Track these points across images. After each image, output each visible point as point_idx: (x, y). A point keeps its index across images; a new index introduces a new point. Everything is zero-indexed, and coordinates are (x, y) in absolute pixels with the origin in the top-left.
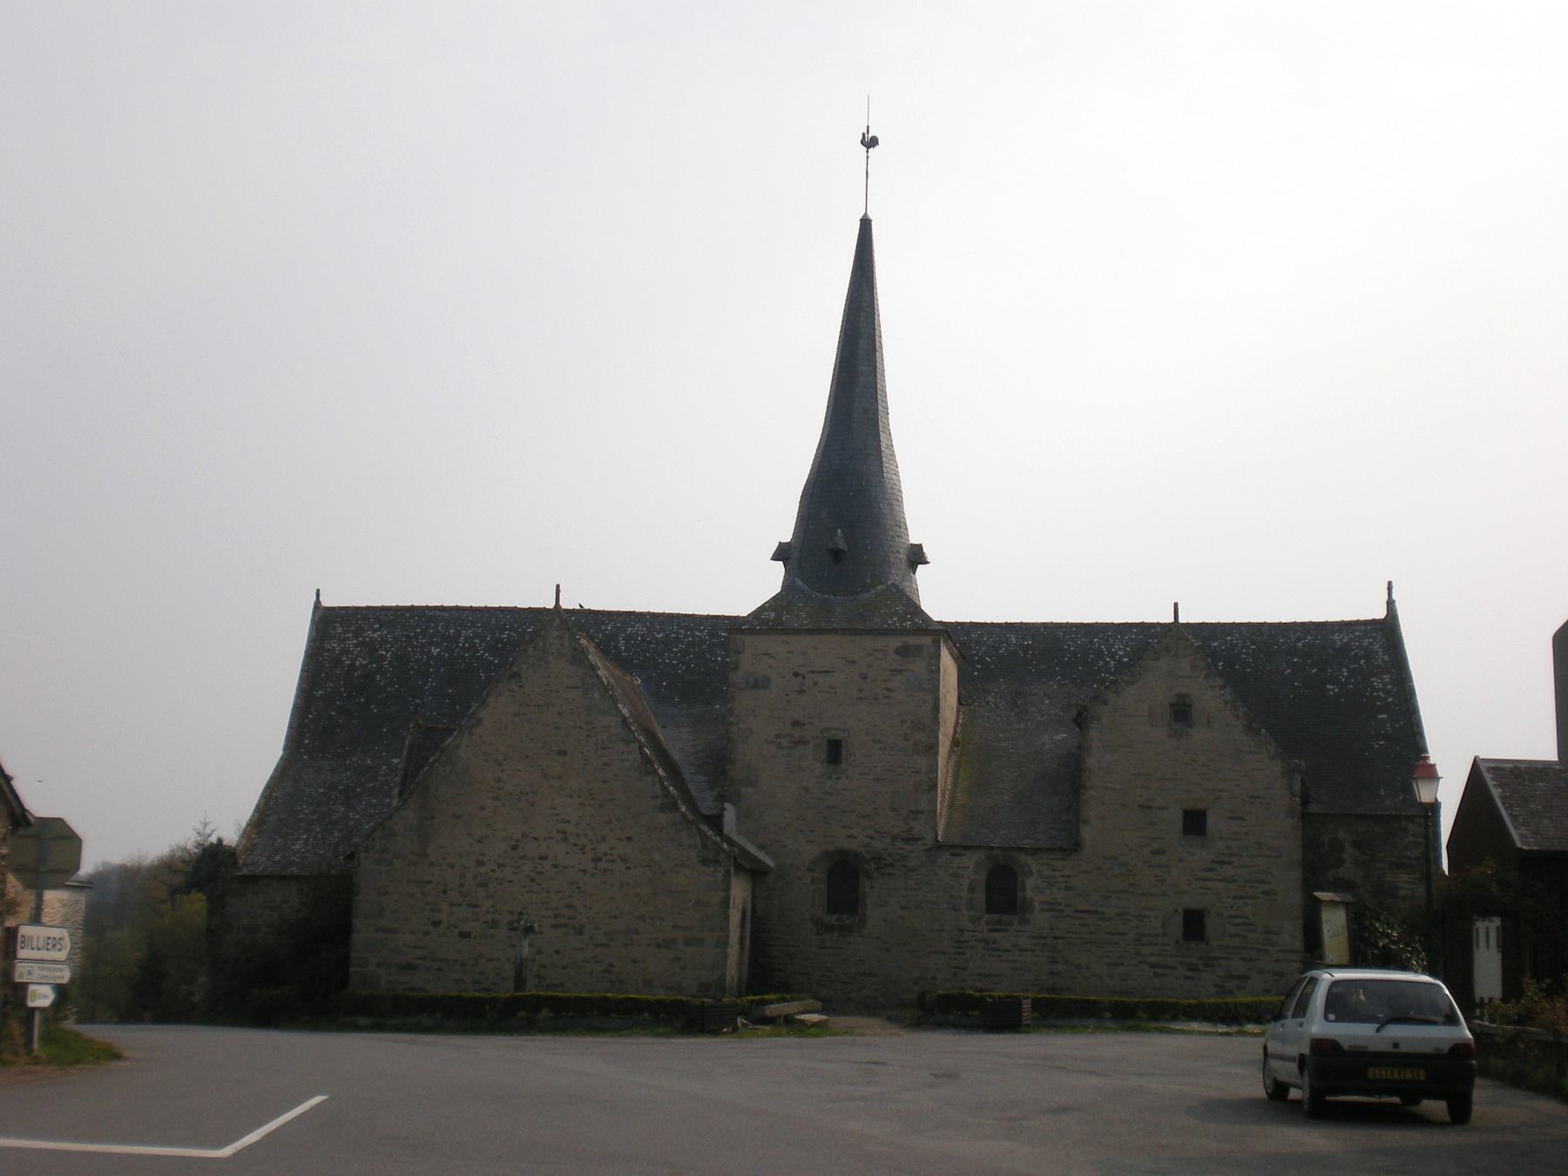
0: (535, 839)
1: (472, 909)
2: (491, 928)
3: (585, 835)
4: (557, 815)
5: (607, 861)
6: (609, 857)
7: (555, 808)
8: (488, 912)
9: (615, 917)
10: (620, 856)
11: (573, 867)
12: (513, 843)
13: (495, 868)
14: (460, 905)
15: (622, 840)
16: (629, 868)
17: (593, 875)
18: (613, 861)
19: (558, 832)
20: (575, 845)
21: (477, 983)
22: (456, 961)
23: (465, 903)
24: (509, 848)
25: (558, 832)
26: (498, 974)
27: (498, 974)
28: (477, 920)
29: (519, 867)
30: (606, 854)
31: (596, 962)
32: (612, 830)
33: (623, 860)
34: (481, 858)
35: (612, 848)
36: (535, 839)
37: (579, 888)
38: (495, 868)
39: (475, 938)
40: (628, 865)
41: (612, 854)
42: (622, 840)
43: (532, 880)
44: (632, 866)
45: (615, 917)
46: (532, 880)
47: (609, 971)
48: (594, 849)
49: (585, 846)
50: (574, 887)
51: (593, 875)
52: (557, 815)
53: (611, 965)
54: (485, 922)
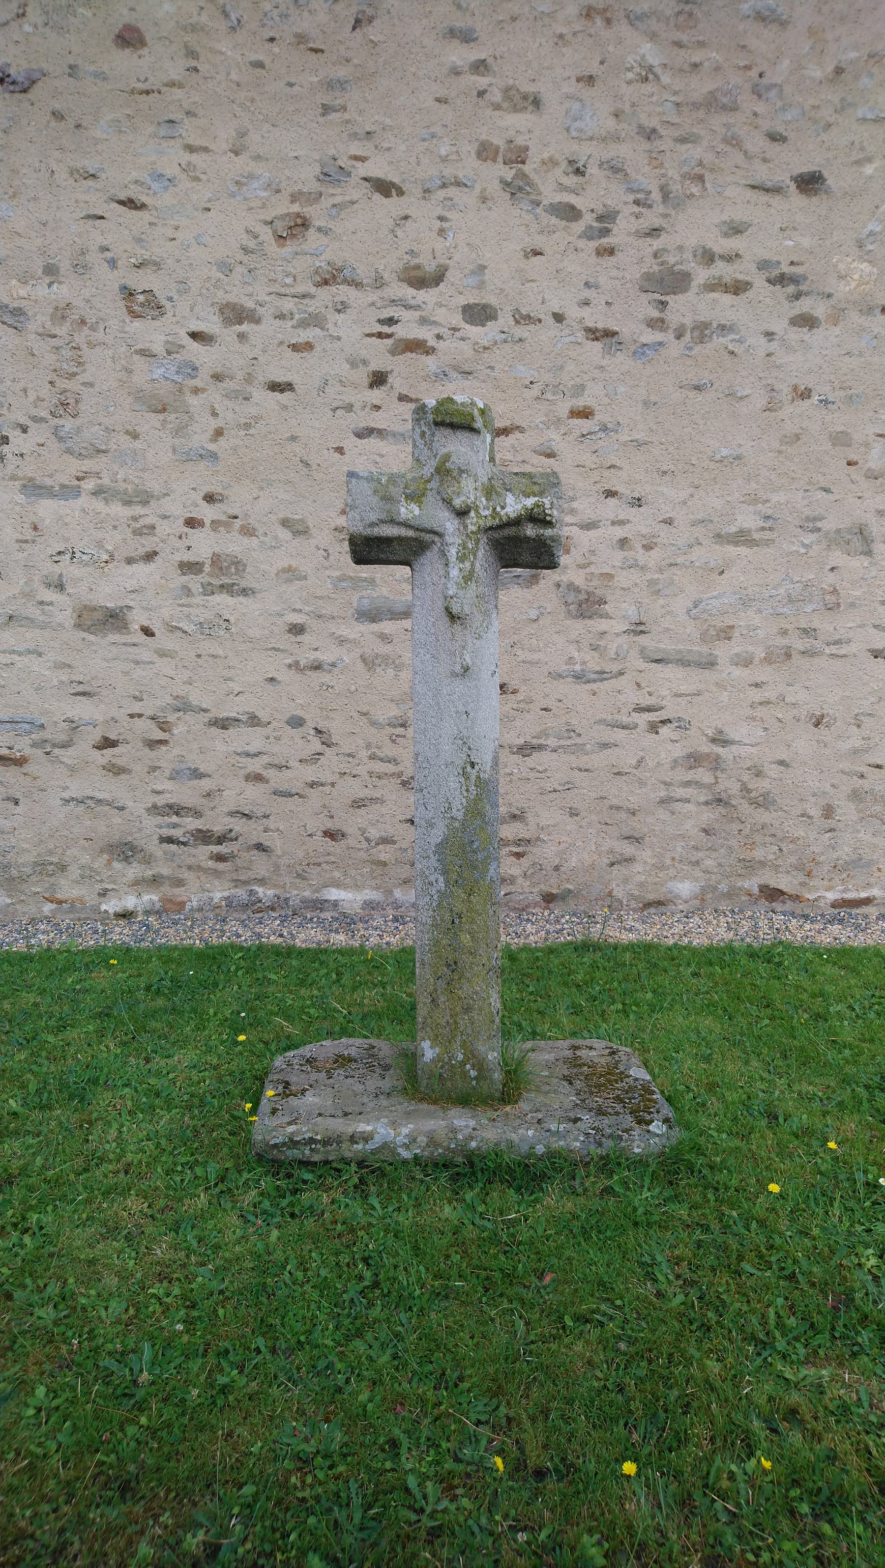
0: (384, 188)
1: (117, 509)
2: (209, 590)
3: (615, 169)
4: (480, 67)
5: (710, 287)
6: (721, 269)
7: (467, 37)
8: (191, 523)
9: (742, 538)
10: (763, 265)
11: (559, 318)
12: (283, 207)
13: (211, 324)
14: (68, 492)
15: (776, 190)
16: (807, 321)
17: (642, 350)
18: (738, 288)
19: (486, 152)
20: (570, 213)
21: (176, 810)
22: (74, 726)
23: (89, 485)
24: (266, 234)
25: (486, 152)
26: (258, 778)
27: (258, 778)
28: (150, 556)
29: (315, 320)
30: (708, 257)
31: (653, 728)
32: (734, 141)
33: (781, 280)
34: (141, 281)
35: (735, 229)
36: (384, 188)
37: (585, 414)
38: (211, 324)
39: (147, 632)
40: (805, 305)
41: (730, 258)
42: (776, 190)
43: (379, 379)
44: (820, 310)
45: (742, 538)
46: (379, 379)
47: (716, 765)
48: (654, 232)
49: (607, 217)
50: (563, 408)
51: (642, 350)
52: (480, 67)
53: (720, 739)
54: (189, 567)
